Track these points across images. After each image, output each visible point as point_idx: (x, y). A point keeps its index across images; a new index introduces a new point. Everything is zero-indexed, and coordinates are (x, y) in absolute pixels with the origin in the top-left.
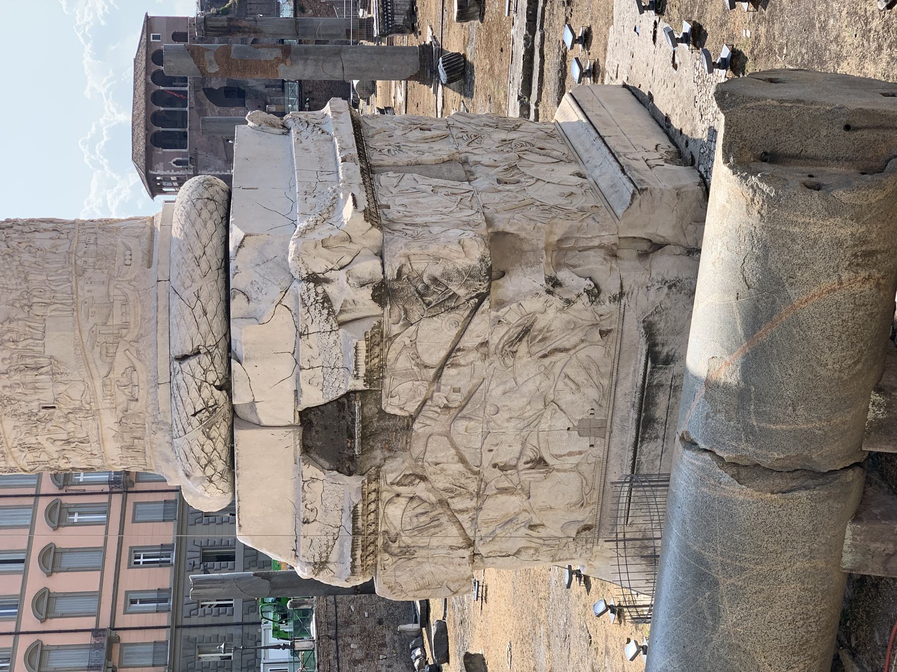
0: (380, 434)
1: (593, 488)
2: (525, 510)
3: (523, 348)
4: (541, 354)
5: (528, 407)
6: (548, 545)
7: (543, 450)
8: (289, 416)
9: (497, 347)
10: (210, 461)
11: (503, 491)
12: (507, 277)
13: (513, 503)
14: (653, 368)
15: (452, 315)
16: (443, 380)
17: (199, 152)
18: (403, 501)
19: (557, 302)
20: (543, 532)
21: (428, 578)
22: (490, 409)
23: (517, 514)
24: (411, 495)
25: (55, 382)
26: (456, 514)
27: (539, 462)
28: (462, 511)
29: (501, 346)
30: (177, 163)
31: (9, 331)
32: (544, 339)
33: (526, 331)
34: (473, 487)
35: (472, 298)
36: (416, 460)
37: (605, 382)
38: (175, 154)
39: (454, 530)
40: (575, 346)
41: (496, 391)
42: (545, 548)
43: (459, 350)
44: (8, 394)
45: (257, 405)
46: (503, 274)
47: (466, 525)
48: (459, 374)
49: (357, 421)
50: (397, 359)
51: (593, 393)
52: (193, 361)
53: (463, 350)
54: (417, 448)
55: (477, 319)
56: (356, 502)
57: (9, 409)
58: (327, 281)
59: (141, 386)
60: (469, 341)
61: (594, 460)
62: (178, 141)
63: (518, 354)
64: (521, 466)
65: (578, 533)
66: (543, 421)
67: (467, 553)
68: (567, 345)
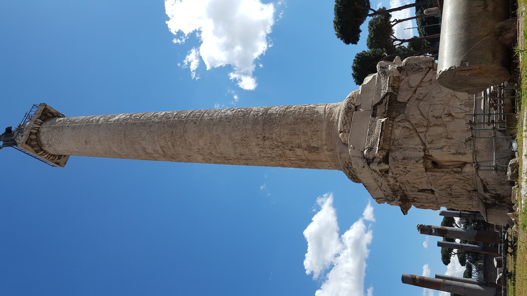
13: (440, 130)
18: (400, 128)
20: (452, 141)
21: (407, 155)
24: (403, 126)
26: (419, 133)
27: (450, 115)
28: (421, 132)
34: (425, 123)
35: (427, 68)
39: (418, 139)
43: (422, 82)
45: (362, 104)
60: (426, 79)
67: (422, 147)
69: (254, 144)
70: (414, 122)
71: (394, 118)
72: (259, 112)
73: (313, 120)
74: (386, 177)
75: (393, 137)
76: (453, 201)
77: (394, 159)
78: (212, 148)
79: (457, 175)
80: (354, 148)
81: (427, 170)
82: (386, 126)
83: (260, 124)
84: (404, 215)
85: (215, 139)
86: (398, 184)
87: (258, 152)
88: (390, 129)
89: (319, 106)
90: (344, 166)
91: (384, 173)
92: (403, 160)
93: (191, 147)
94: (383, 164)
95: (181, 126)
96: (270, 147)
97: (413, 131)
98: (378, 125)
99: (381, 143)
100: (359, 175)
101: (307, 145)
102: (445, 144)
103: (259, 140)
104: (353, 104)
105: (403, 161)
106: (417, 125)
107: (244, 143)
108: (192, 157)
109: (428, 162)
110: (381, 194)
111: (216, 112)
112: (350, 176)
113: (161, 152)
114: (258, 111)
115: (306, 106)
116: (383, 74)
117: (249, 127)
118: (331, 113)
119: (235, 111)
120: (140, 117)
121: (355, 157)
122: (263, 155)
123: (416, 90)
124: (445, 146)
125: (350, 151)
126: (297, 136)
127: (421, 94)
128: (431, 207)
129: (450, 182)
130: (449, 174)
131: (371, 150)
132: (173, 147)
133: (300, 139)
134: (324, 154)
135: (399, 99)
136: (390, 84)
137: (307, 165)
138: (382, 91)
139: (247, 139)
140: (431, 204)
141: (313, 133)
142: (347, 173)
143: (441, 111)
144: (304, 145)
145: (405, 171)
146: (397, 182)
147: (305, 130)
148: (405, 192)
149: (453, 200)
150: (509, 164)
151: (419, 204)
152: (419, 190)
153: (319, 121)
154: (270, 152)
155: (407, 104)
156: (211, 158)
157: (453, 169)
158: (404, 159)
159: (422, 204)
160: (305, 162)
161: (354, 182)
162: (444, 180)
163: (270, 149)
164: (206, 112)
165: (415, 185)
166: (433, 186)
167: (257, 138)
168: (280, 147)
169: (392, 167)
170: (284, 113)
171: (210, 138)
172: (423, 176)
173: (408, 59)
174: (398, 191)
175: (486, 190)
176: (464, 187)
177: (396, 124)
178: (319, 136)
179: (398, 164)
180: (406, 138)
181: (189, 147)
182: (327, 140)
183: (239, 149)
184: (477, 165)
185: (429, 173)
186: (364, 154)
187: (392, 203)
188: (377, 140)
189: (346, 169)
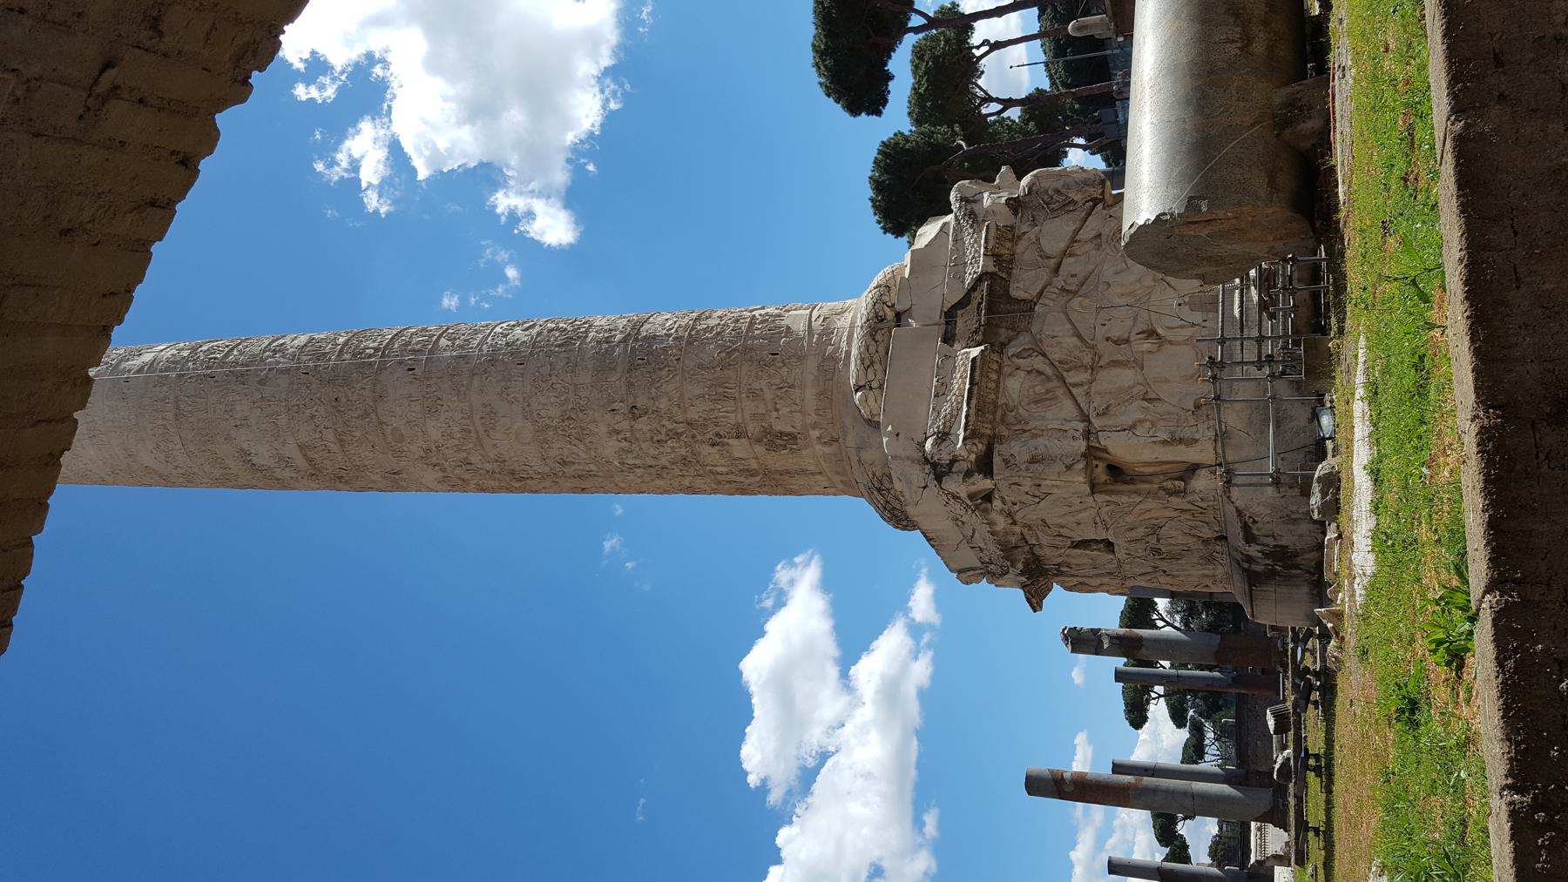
10: (872, 363)
13: (1127, 376)
18: (1022, 374)
20: (1160, 407)
21: (1041, 450)
23: (1131, 388)
24: (1029, 369)
26: (1071, 388)
27: (1151, 333)
28: (1076, 385)
29: (1111, 234)
34: (1087, 360)
35: (1086, 202)
39: (1068, 403)
43: (1076, 241)
48: (1076, 262)
53: (1079, 241)
60: (1085, 234)
67: (1081, 426)
69: (604, 430)
70: (1056, 356)
71: (1004, 345)
72: (614, 333)
73: (777, 354)
74: (985, 511)
75: (1003, 401)
76: (1165, 569)
77: (1006, 462)
78: (471, 446)
79: (1174, 500)
80: (897, 435)
81: (1094, 488)
82: (982, 370)
83: (620, 369)
84: (1035, 612)
85: (478, 417)
86: (1017, 529)
87: (615, 453)
88: (994, 376)
89: (791, 313)
90: (870, 485)
91: (979, 501)
92: (1032, 465)
93: (399, 445)
94: (977, 477)
95: (365, 381)
96: (652, 438)
97: (1055, 383)
98: (962, 365)
99: (972, 418)
100: (911, 510)
101: (762, 429)
102: (1142, 417)
103: (619, 418)
104: (890, 305)
105: (1033, 467)
106: (1067, 363)
107: (571, 429)
108: (405, 476)
109: (1097, 466)
110: (970, 558)
111: (476, 332)
112: (886, 513)
113: (300, 462)
114: (611, 330)
115: (754, 313)
116: (970, 218)
117: (585, 378)
118: (827, 332)
119: (537, 329)
120: (227, 355)
121: (902, 459)
122: (631, 462)
123: (1060, 264)
124: (1142, 421)
125: (887, 442)
126: (732, 403)
127: (1072, 276)
128: (1105, 588)
129: (1157, 519)
130: (1154, 498)
131: (944, 440)
132: (343, 446)
133: (742, 409)
134: (814, 453)
135: (1016, 292)
136: (990, 247)
137: (765, 485)
138: (969, 269)
139: (581, 414)
140: (1106, 580)
142: (880, 505)
143: (1129, 323)
144: (753, 428)
145: (1037, 493)
146: (1014, 523)
147: (756, 385)
148: (1037, 551)
149: (1164, 565)
150: (1316, 476)
151: (1075, 581)
152: (1075, 544)
154: (652, 452)
155: (1035, 304)
156: (467, 477)
157: (1164, 484)
158: (1033, 461)
159: (1080, 580)
160: (758, 479)
161: (897, 528)
162: (1143, 513)
163: (653, 443)
164: (444, 332)
165: (1063, 531)
166: (1110, 531)
167: (613, 410)
168: (683, 438)
169: (1003, 485)
170: (689, 334)
171: (462, 415)
172: (1084, 506)
173: (1034, 176)
174: (1016, 547)
175: (1249, 538)
176: (1193, 532)
177: (1009, 363)
178: (797, 402)
179: (1019, 477)
180: (1037, 402)
181: (394, 443)
182: (820, 412)
183: (557, 445)
184: (1228, 472)
185: (1100, 498)
186: (924, 451)
187: (1001, 582)
188: (959, 409)
189: (875, 493)
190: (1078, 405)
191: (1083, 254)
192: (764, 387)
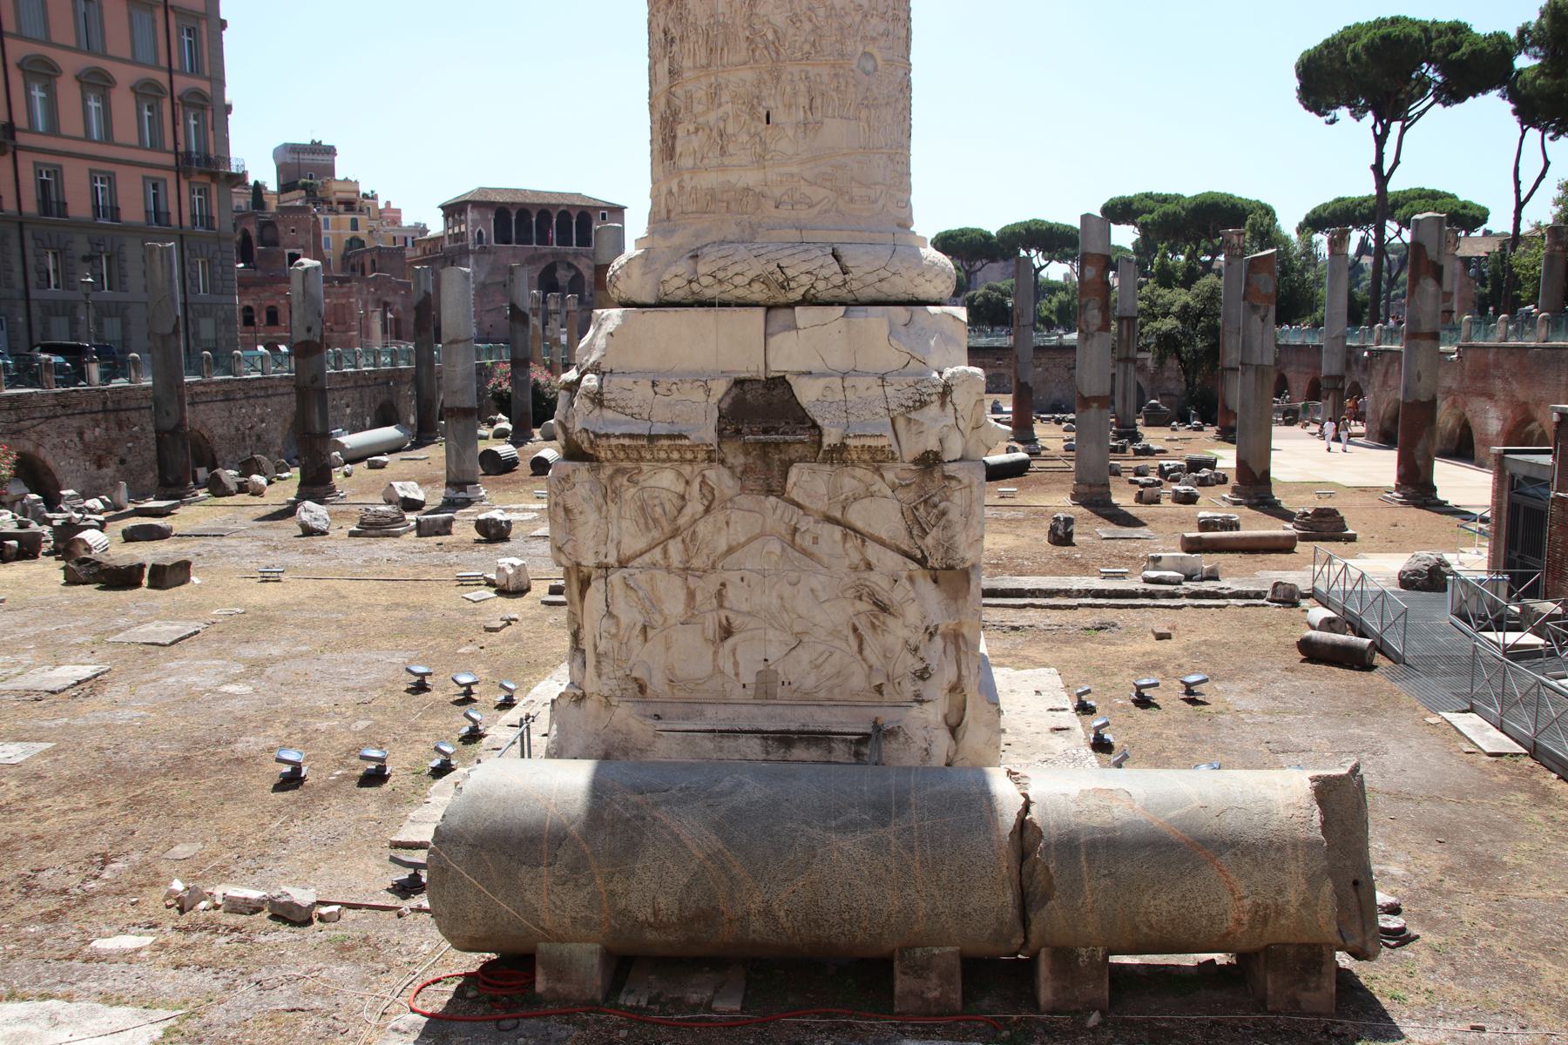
0: (764, 462)
1: (693, 691)
2: (665, 621)
3: (865, 606)
4: (857, 624)
5: (794, 616)
6: (620, 648)
7: (743, 635)
8: (778, 366)
9: (866, 579)
10: (720, 282)
11: (691, 595)
12: (933, 586)
13: (675, 606)
14: (851, 741)
15: (904, 533)
16: (828, 526)
17: (492, 257)
18: (680, 488)
19: (918, 637)
20: (636, 641)
21: (580, 519)
22: (794, 576)
23: (661, 612)
25: (797, 125)
27: (727, 632)
28: (665, 552)
30: (480, 233)
31: (847, 83)
32: (874, 626)
33: (884, 608)
34: (697, 563)
35: (922, 552)
36: (731, 500)
37: (822, 694)
38: (489, 230)
39: (641, 544)
40: (864, 660)
41: (817, 581)
42: (616, 645)
44: (783, 77)
46: (935, 581)
47: (647, 558)
48: (835, 542)
49: (787, 438)
50: (854, 477)
51: (810, 682)
52: (836, 268)
53: (863, 545)
54: (745, 501)
55: (899, 558)
56: (692, 437)
57: (767, 77)
58: (943, 404)
59: (794, 213)
60: (873, 552)
61: (728, 690)
62: (503, 236)
63: (858, 602)
64: (723, 613)
65: (636, 679)
66: (778, 633)
67: (612, 560)
68: (867, 652)
70: (703, 529)
73: (768, 122)
97: (667, 528)
124: (618, 625)
141: (715, 133)
143: (745, 607)
147: (726, 96)
153: (765, 150)
177: (696, 473)
178: (706, 161)
180: (642, 509)
190: (641, 554)
191: (845, 550)
192: (722, 109)
